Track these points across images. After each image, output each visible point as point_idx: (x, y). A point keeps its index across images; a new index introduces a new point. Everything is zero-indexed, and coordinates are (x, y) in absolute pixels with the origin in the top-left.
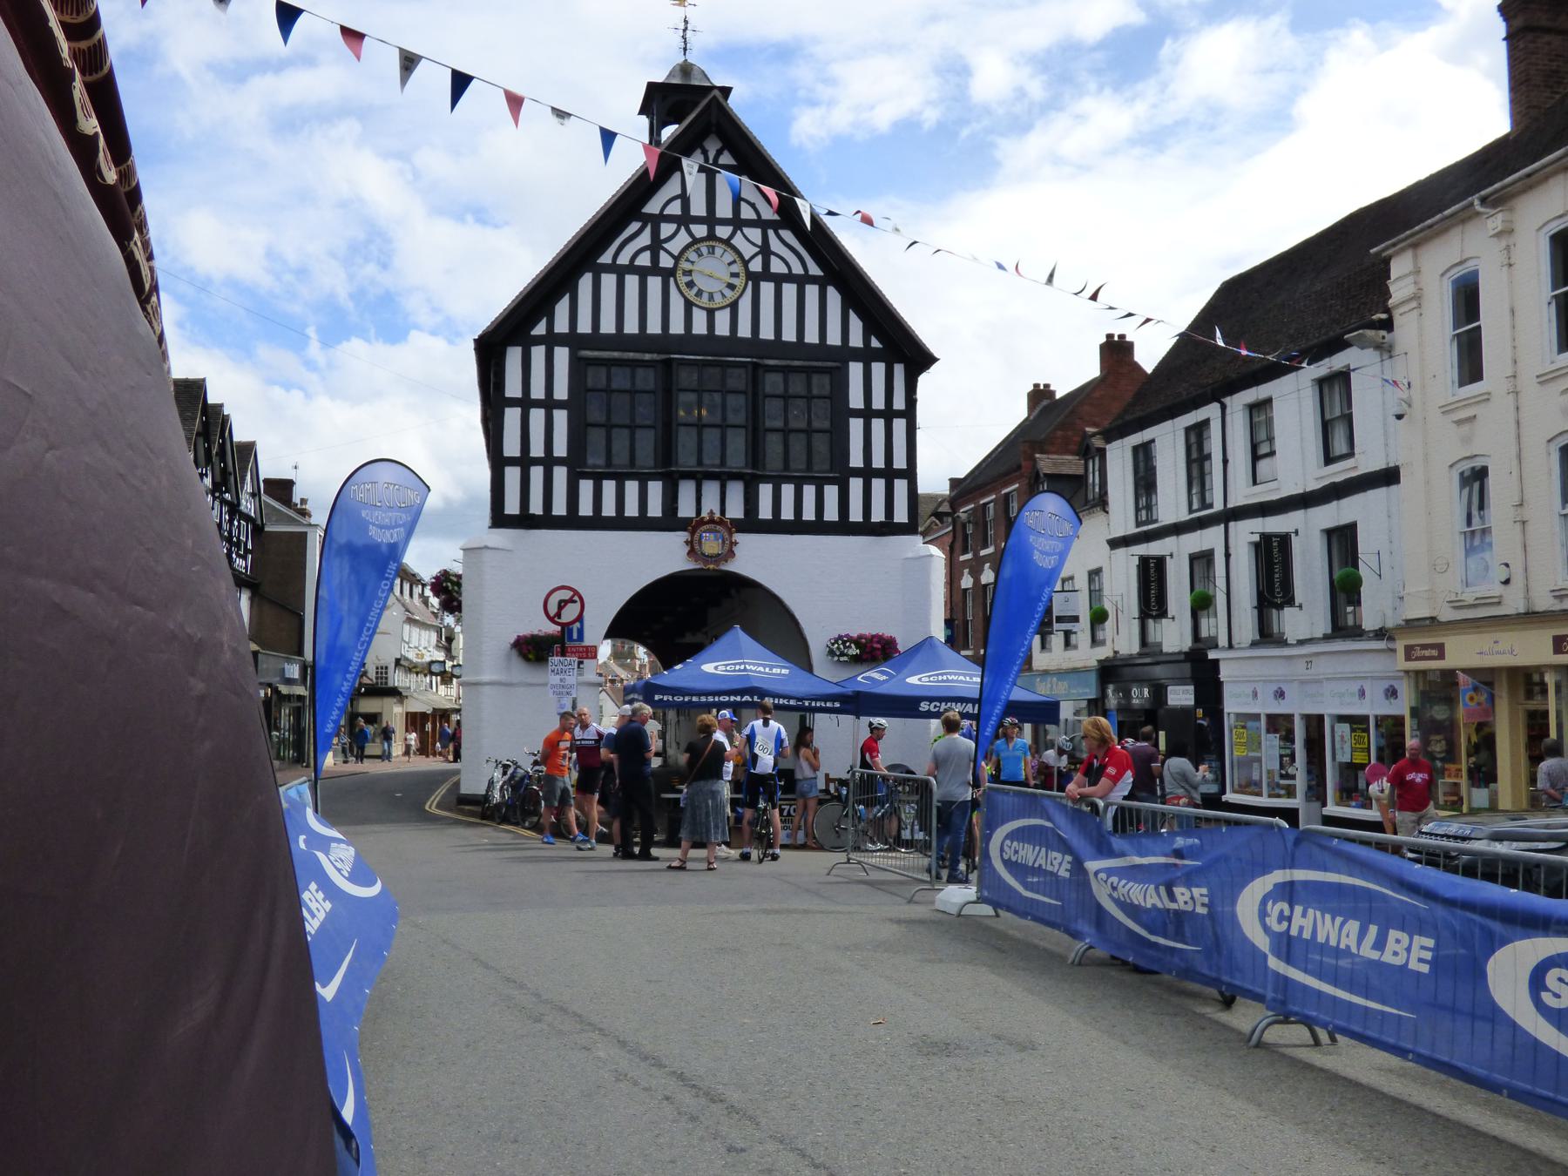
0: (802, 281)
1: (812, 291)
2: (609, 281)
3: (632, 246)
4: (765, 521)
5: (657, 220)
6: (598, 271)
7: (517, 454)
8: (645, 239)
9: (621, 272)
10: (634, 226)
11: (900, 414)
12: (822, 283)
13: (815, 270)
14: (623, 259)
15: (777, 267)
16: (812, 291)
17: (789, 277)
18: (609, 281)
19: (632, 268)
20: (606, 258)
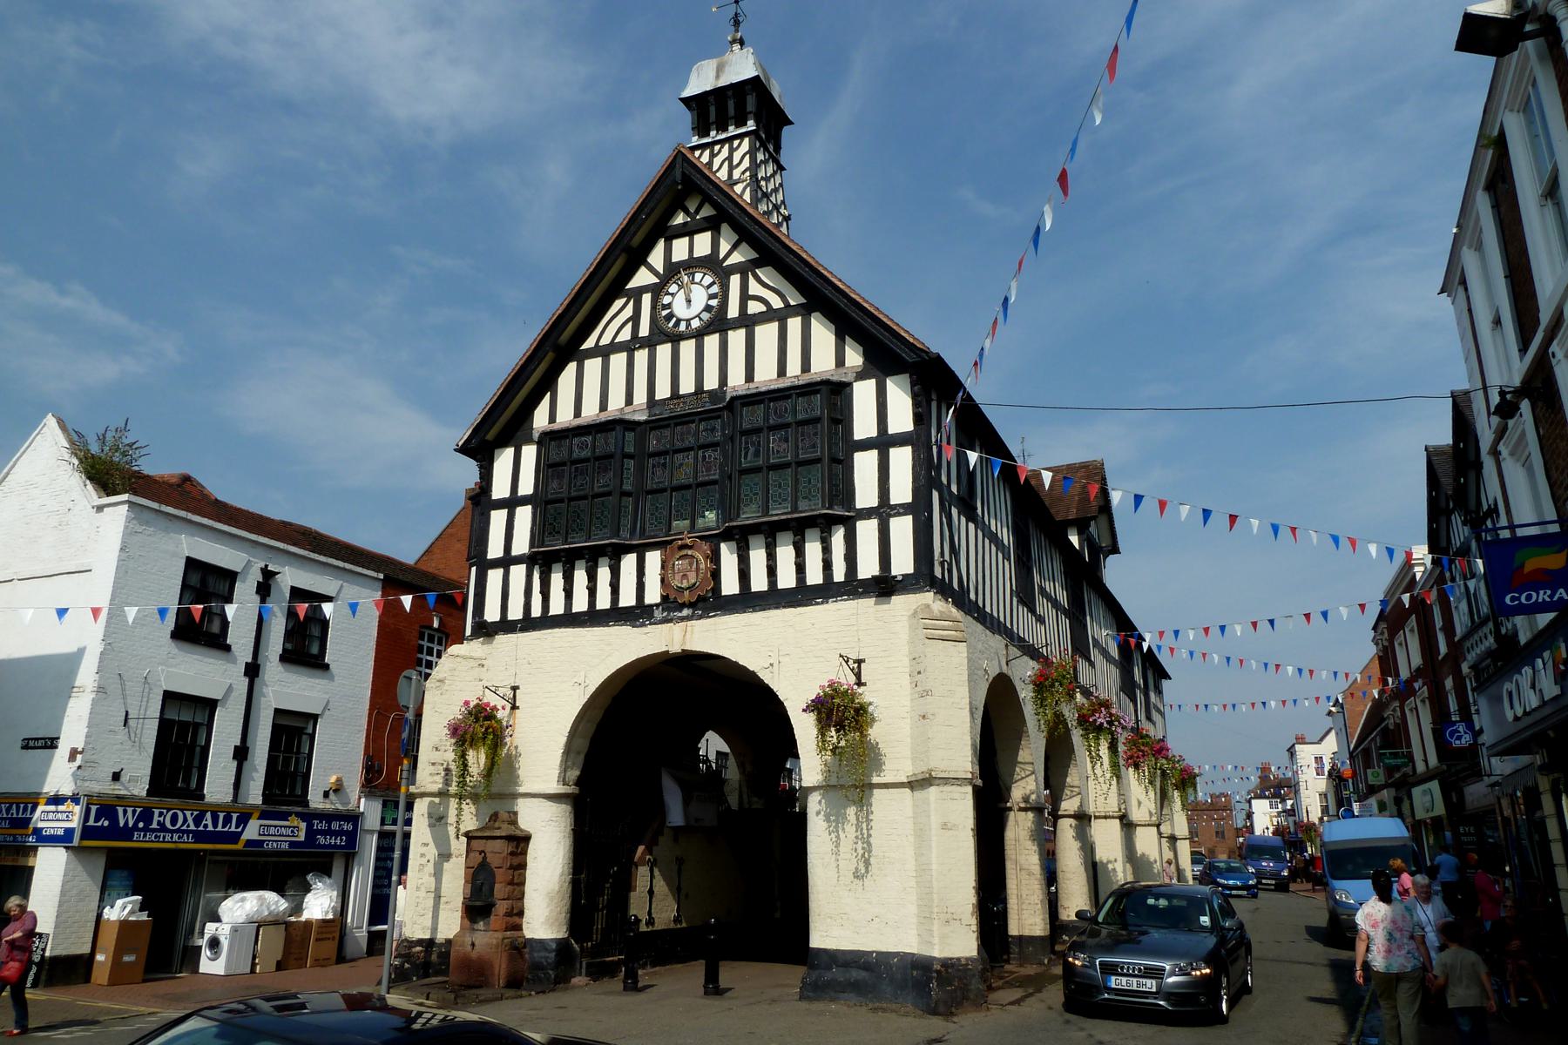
0: (780, 317)
1: (794, 324)
2: (593, 366)
3: (615, 325)
8: (629, 312)
9: (604, 352)
10: (618, 303)
11: (901, 440)
12: (805, 311)
13: (795, 299)
14: (605, 341)
15: (754, 308)
16: (794, 324)
17: (770, 315)
19: (614, 348)
20: (589, 343)
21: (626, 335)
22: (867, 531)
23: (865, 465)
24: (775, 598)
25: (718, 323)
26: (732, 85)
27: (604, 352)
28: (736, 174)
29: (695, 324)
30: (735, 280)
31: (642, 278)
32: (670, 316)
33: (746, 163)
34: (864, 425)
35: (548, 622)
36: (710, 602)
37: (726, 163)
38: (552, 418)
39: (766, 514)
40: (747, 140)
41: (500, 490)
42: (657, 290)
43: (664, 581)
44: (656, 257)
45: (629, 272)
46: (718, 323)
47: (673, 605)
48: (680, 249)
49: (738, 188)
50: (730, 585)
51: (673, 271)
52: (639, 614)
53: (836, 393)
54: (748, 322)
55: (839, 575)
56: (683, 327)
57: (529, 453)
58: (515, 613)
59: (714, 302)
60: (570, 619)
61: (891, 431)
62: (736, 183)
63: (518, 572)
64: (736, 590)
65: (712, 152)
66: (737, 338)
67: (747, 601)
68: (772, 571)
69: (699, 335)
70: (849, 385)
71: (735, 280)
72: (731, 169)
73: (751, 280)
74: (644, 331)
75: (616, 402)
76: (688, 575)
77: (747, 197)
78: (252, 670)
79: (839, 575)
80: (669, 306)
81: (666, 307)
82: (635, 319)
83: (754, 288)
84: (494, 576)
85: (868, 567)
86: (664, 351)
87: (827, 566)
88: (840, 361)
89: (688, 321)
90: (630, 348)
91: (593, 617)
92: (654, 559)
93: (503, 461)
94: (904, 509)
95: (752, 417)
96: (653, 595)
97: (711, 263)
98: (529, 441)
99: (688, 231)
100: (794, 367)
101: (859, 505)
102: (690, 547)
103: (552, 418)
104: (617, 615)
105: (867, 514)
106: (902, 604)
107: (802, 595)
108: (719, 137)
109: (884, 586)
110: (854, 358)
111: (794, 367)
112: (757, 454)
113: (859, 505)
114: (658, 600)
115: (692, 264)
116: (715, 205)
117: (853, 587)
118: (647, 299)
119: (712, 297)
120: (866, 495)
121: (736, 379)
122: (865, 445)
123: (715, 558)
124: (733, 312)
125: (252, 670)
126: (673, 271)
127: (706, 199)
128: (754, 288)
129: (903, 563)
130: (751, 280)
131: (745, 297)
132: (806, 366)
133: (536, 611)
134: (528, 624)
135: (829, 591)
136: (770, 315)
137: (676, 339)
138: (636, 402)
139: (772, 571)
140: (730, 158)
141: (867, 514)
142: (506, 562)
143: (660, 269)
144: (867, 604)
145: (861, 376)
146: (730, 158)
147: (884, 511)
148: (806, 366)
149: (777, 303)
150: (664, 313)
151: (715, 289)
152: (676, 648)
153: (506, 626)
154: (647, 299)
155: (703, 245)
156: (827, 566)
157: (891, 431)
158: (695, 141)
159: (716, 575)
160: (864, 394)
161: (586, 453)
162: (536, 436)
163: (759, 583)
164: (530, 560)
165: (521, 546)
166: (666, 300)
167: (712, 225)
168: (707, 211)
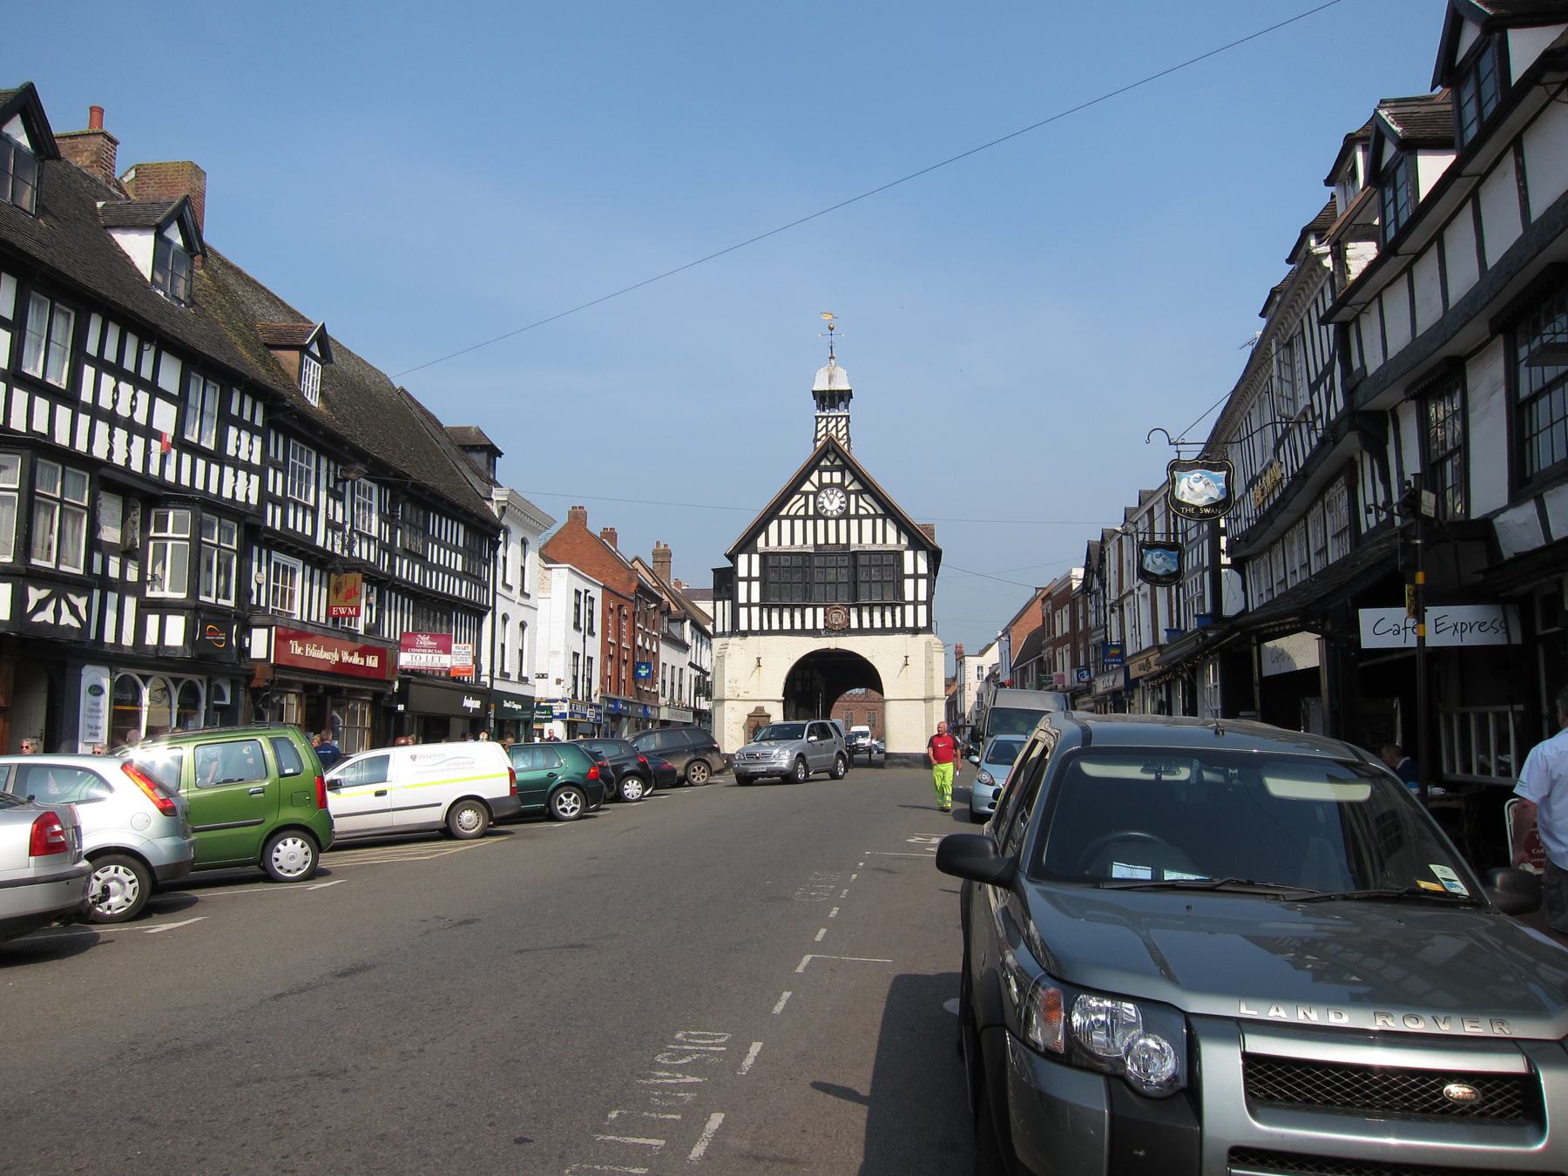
0: (874, 517)
2: (786, 524)
3: (796, 505)
4: (866, 629)
5: (806, 494)
6: (780, 519)
7: (746, 601)
8: (802, 501)
9: (793, 518)
10: (797, 497)
13: (880, 511)
14: (792, 513)
15: (862, 512)
16: (879, 522)
17: (868, 516)
18: (786, 524)
20: (784, 512)
21: (802, 512)
22: (909, 609)
23: (909, 584)
24: (872, 631)
25: (846, 515)
26: (838, 391)
27: (796, 517)
28: (840, 435)
29: (835, 513)
30: (853, 497)
31: (807, 487)
32: (823, 507)
33: (844, 431)
34: (908, 569)
35: (770, 632)
36: (846, 631)
37: (835, 428)
38: (767, 544)
39: (871, 600)
40: (844, 419)
41: (742, 572)
42: (816, 495)
43: (825, 620)
44: (815, 477)
45: (802, 483)
46: (846, 515)
47: (830, 631)
48: (826, 477)
49: (842, 442)
50: (854, 624)
51: (822, 487)
52: (815, 632)
53: (898, 556)
54: (860, 518)
55: (898, 624)
56: (829, 513)
57: (756, 558)
58: (755, 626)
59: (843, 505)
60: (781, 632)
61: (919, 572)
62: (842, 439)
63: (755, 611)
64: (857, 627)
65: (827, 420)
66: (854, 523)
67: (861, 631)
68: (871, 621)
69: (837, 519)
70: (902, 552)
71: (853, 497)
72: (837, 432)
73: (860, 499)
74: (811, 512)
75: (799, 540)
76: (837, 619)
77: (846, 446)
78: (584, 636)
79: (898, 624)
80: (822, 503)
81: (820, 503)
82: (806, 505)
83: (861, 503)
84: (743, 612)
85: (909, 623)
86: (821, 523)
87: (894, 621)
88: (899, 541)
89: (832, 511)
90: (805, 518)
91: (792, 632)
92: (820, 611)
93: (743, 559)
94: (923, 603)
95: (863, 560)
96: (820, 625)
97: (841, 486)
98: (756, 552)
99: (831, 470)
100: (879, 540)
101: (906, 599)
102: (838, 609)
103: (767, 544)
104: (803, 632)
105: (909, 603)
106: (922, 638)
107: (883, 631)
108: (831, 414)
109: (916, 631)
110: (904, 541)
111: (879, 540)
112: (867, 575)
113: (906, 599)
114: (823, 627)
115: (831, 485)
116: (842, 460)
117: (903, 630)
118: (811, 497)
119: (842, 502)
120: (909, 596)
121: (854, 540)
122: (909, 577)
123: (849, 614)
124: (852, 512)
125: (584, 636)
126: (822, 487)
127: (838, 456)
128: (861, 503)
129: (922, 623)
130: (860, 499)
131: (857, 506)
132: (884, 541)
133: (766, 627)
134: (761, 632)
135: (894, 630)
136: (868, 516)
137: (826, 519)
138: (808, 543)
139: (871, 621)
140: (836, 426)
141: (909, 603)
142: (749, 605)
143: (817, 484)
144: (909, 636)
145: (907, 549)
146: (836, 426)
147: (916, 603)
148: (884, 541)
149: (872, 512)
150: (820, 505)
151: (843, 499)
152: (832, 647)
153: (749, 632)
154: (811, 497)
155: (837, 477)
156: (894, 621)
157: (919, 572)
158: (818, 413)
159: (849, 620)
160: (908, 556)
161: (788, 564)
162: (759, 551)
163: (866, 625)
164: (761, 606)
165: (756, 598)
166: (821, 500)
167: (842, 469)
168: (838, 462)
